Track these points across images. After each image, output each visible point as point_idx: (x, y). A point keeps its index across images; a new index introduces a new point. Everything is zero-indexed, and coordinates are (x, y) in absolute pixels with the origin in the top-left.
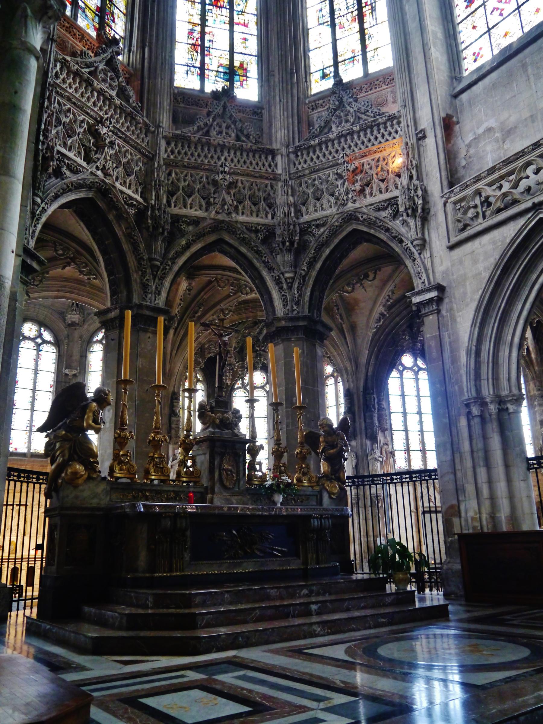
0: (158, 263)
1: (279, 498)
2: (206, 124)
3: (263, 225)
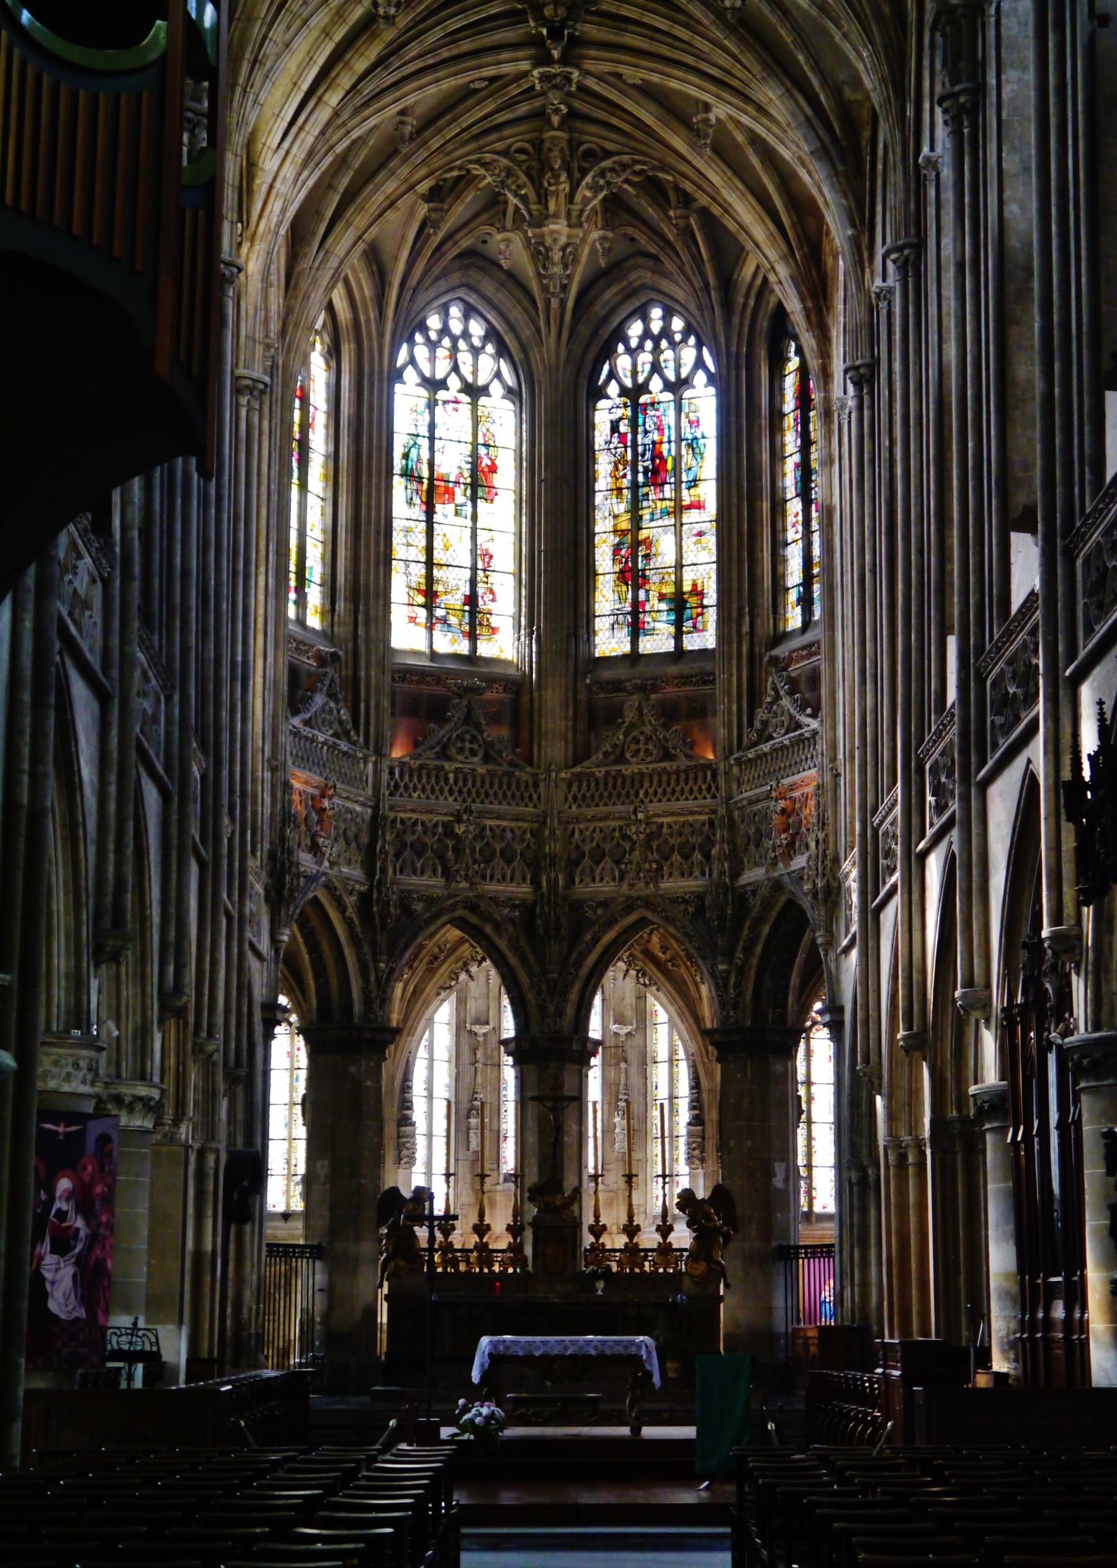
0: (556, 976)
1: (600, 1285)
2: (615, 746)
3: (692, 893)
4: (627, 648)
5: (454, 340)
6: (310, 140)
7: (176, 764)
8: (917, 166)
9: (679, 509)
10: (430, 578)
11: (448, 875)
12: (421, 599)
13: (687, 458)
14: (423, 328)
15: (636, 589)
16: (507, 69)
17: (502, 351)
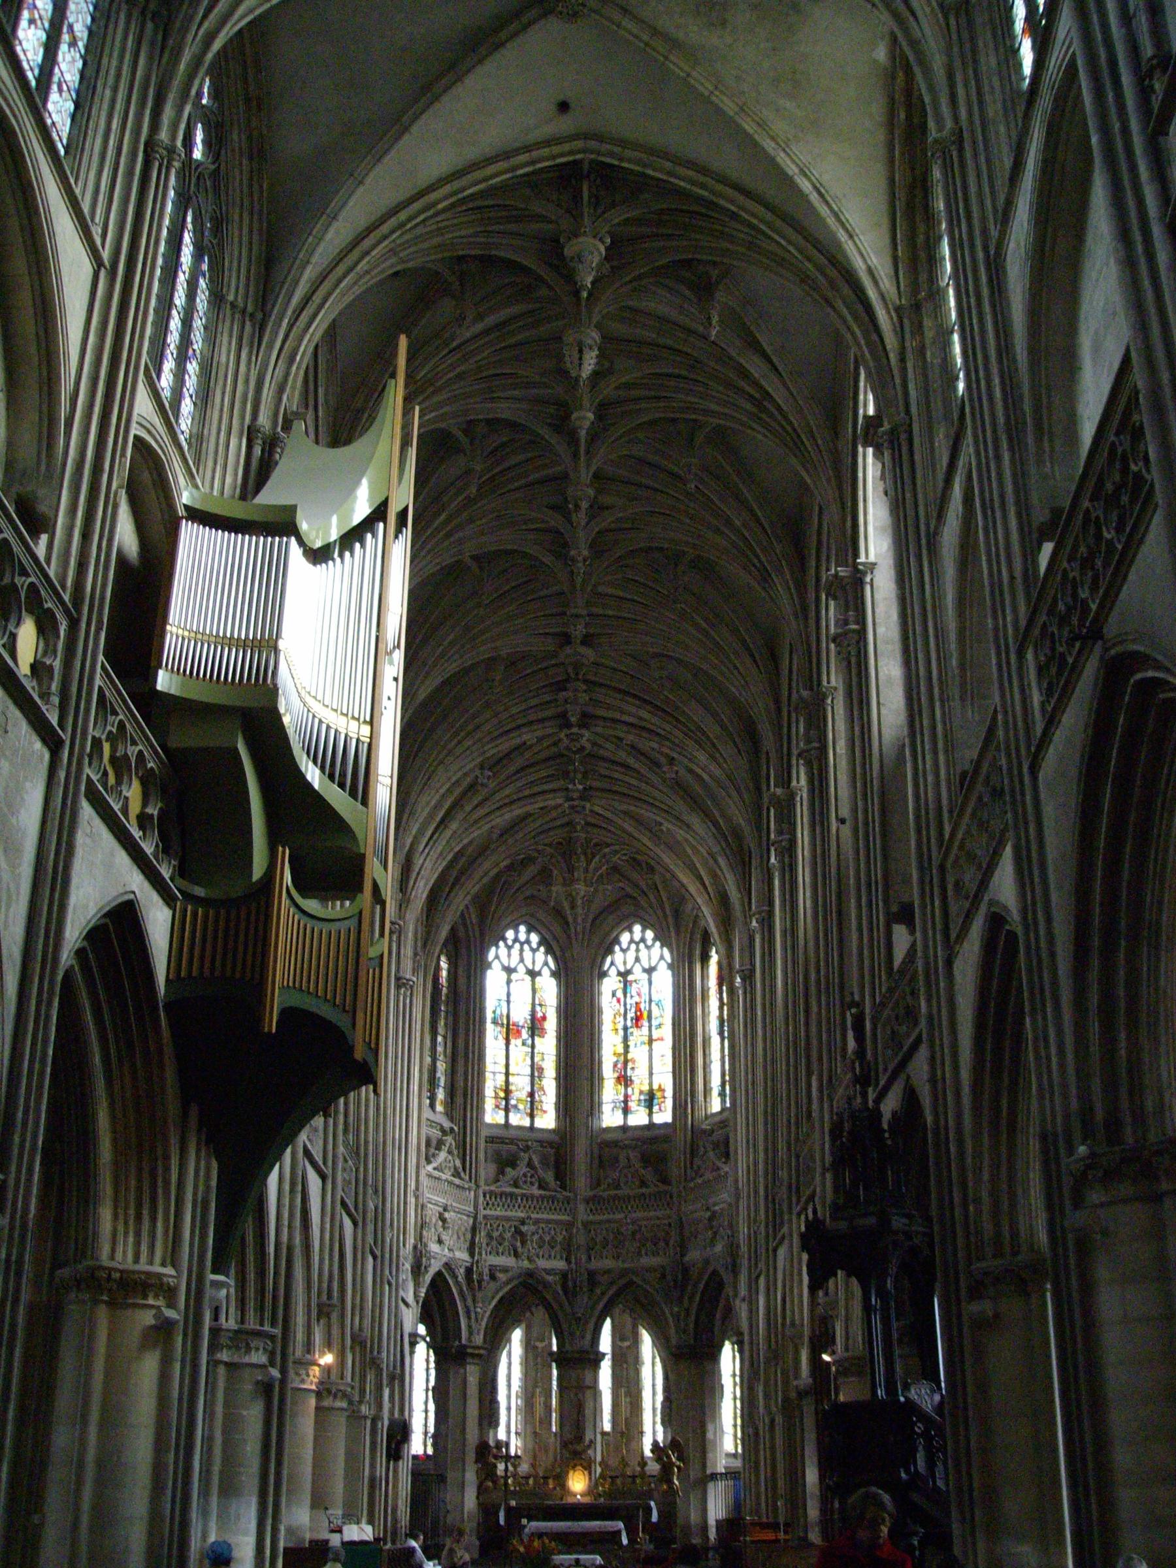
4: (621, 1123)
5: (522, 944)
6: (440, 848)
7: (361, 1206)
8: (769, 870)
9: (651, 1041)
10: (507, 1082)
11: (516, 1255)
12: (502, 1095)
13: (655, 1012)
14: (504, 939)
15: (626, 1086)
16: (552, 803)
17: (549, 950)
